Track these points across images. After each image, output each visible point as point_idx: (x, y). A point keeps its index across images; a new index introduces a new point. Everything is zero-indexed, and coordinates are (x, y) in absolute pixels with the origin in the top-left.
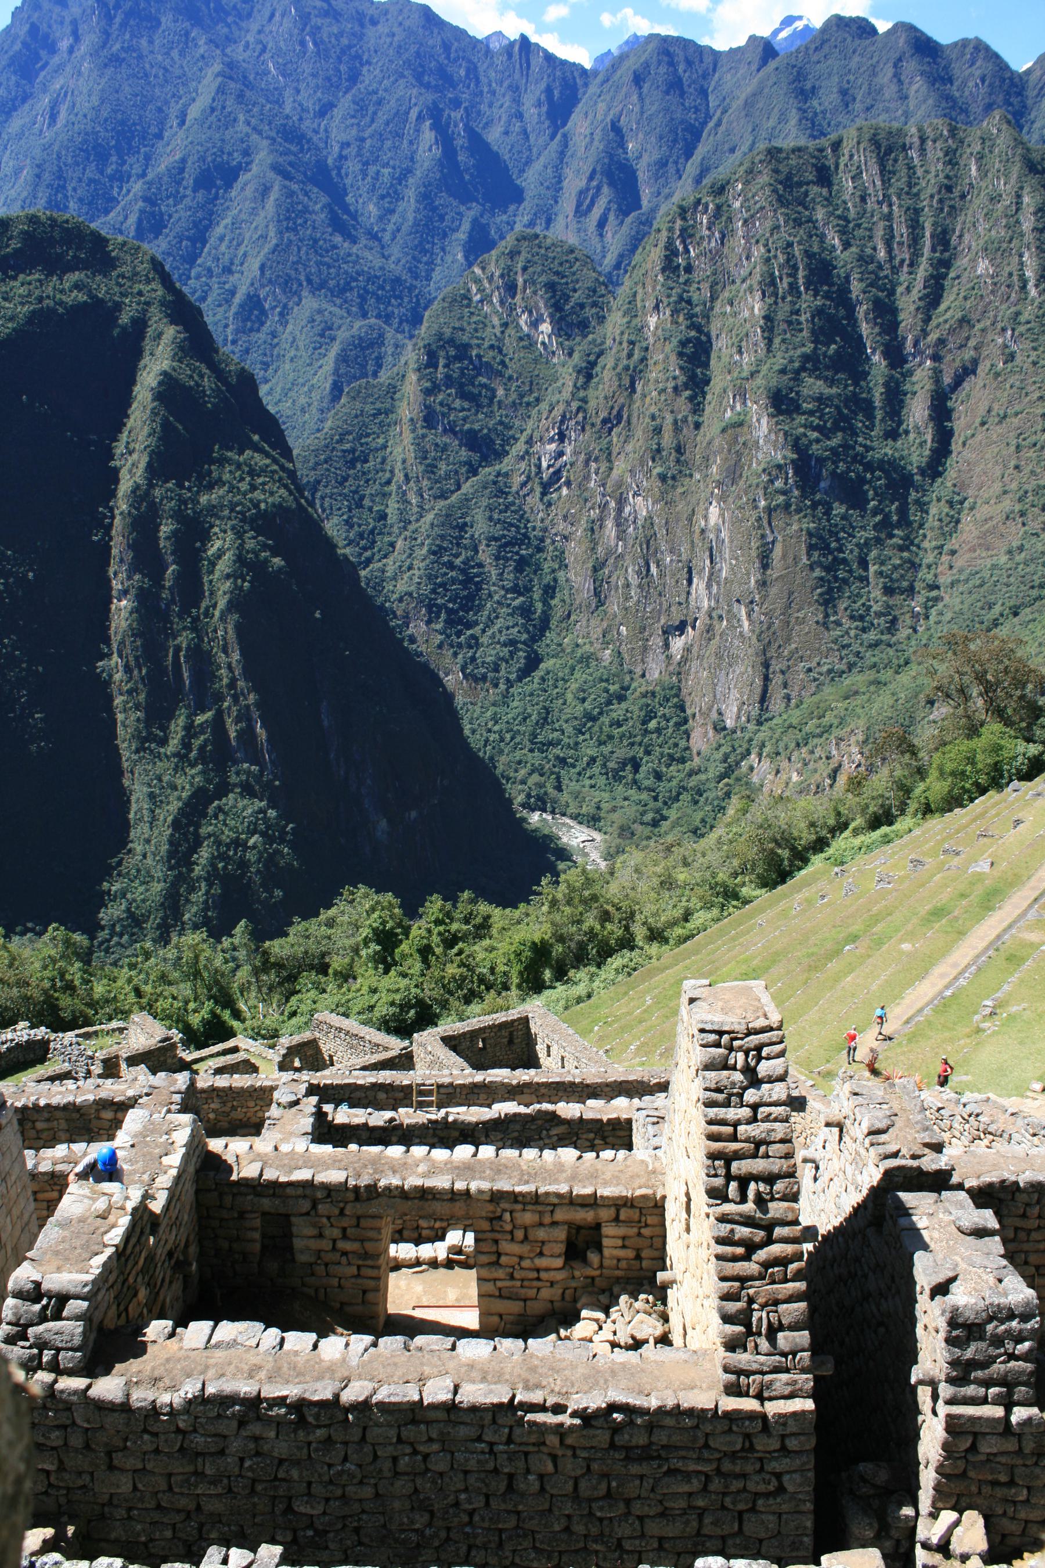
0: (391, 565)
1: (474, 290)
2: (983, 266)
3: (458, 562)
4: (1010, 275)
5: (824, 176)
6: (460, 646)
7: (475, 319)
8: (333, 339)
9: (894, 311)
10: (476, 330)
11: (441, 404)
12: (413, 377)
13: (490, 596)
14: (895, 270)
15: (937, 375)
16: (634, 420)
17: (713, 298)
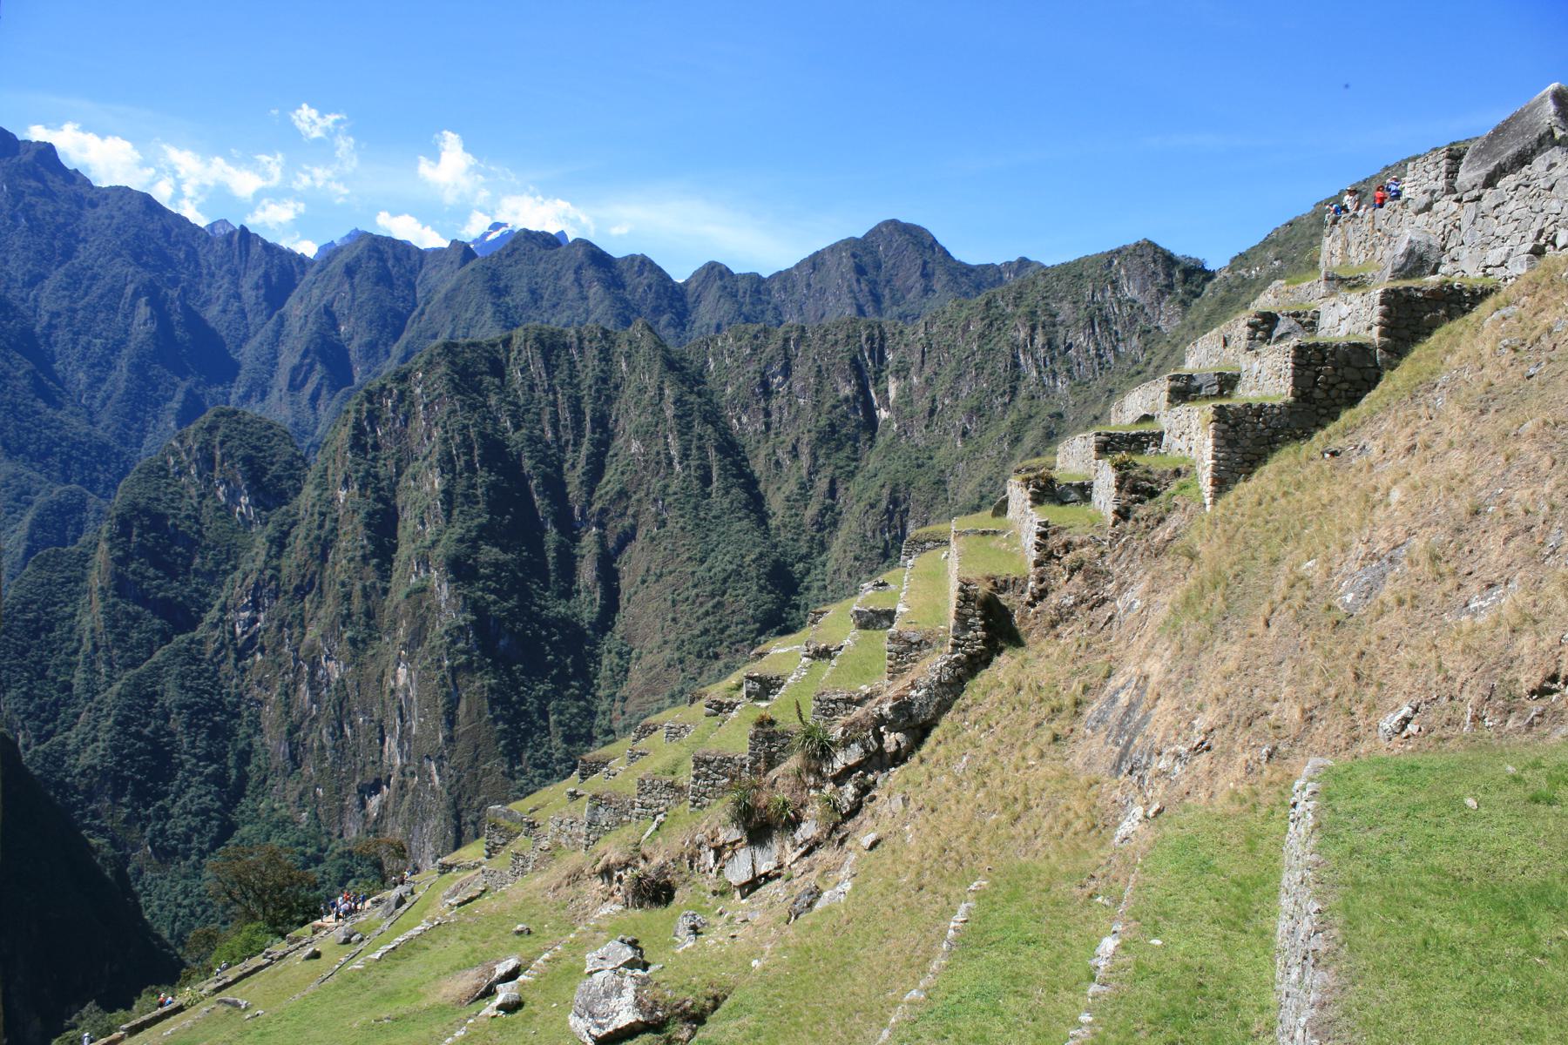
0: (73, 739)
1: (172, 462)
2: (635, 446)
3: (146, 731)
4: (658, 453)
5: (498, 368)
6: (148, 818)
7: (171, 489)
8: (30, 504)
9: (564, 485)
10: (172, 500)
11: (134, 572)
12: (104, 546)
13: (181, 764)
14: (562, 449)
15: (602, 540)
16: (325, 587)
17: (399, 474)
